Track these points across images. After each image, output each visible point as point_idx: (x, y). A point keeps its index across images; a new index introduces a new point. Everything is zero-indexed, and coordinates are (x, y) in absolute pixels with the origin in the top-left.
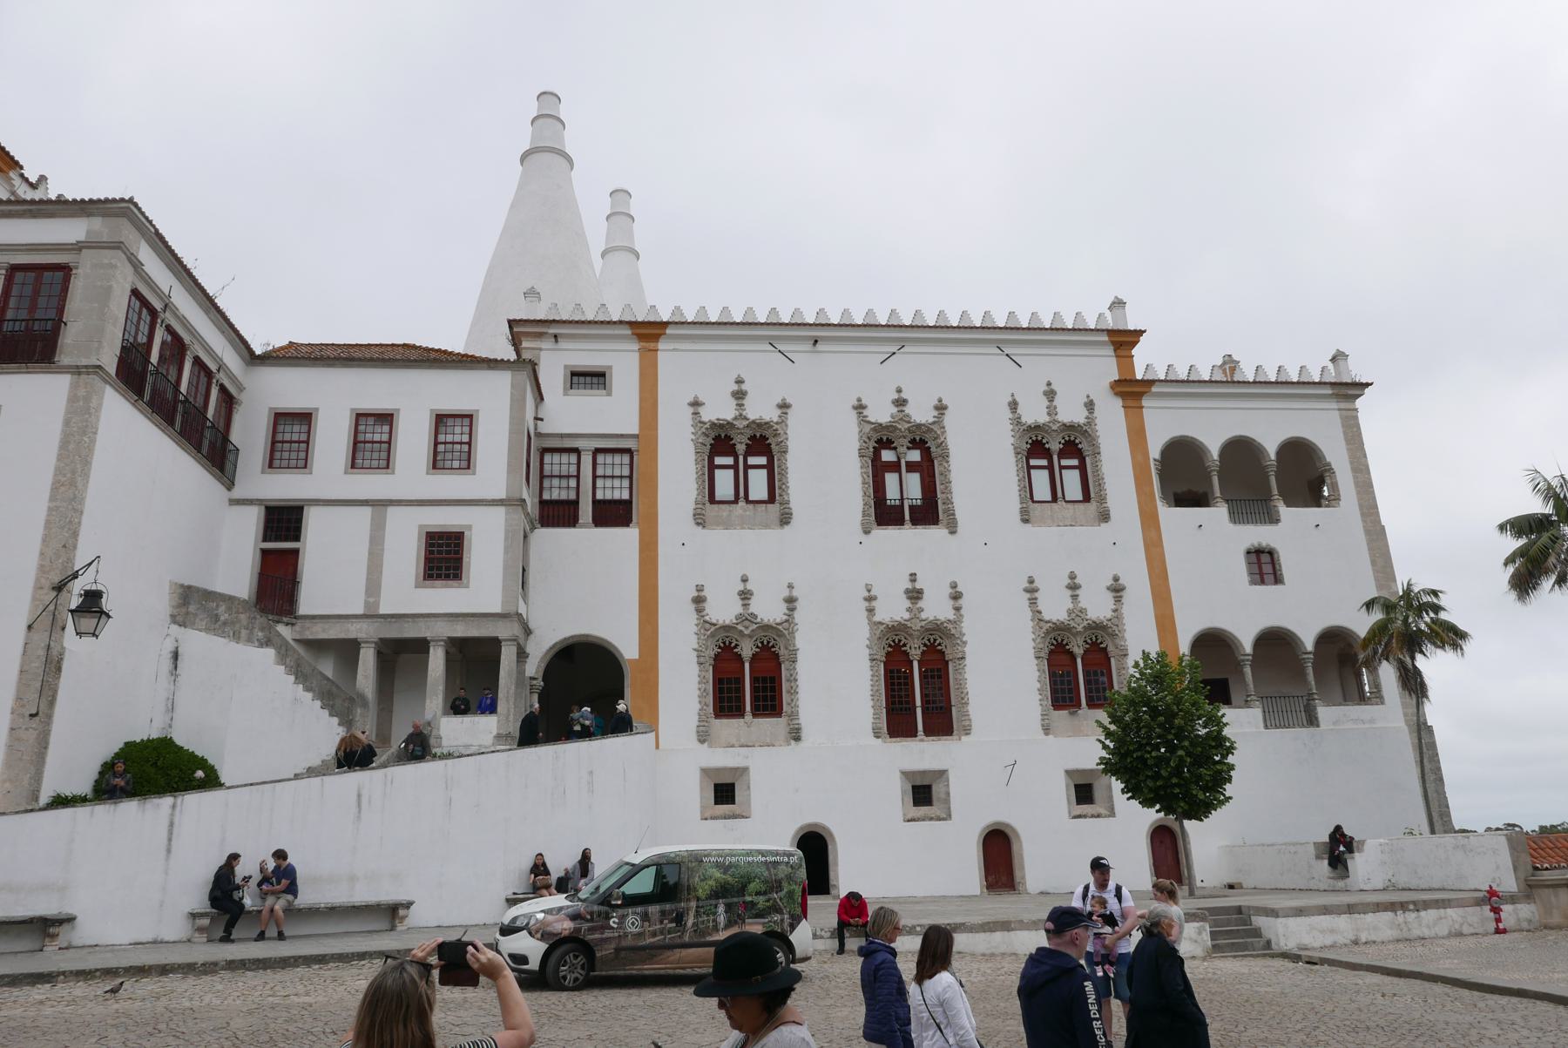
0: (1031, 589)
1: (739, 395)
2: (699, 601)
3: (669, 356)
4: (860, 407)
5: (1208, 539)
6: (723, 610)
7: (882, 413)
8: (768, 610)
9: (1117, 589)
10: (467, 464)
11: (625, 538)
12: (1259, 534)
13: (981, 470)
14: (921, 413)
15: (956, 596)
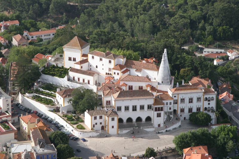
0: (197, 106)
1: (183, 97)
2: (180, 107)
3: (179, 95)
4: (189, 97)
5: (207, 102)
6: (181, 108)
7: (190, 97)
8: (183, 108)
9: (201, 106)
10: (171, 104)
11: (177, 105)
12: (209, 102)
13: (195, 100)
14: (192, 97)
15: (193, 107)
